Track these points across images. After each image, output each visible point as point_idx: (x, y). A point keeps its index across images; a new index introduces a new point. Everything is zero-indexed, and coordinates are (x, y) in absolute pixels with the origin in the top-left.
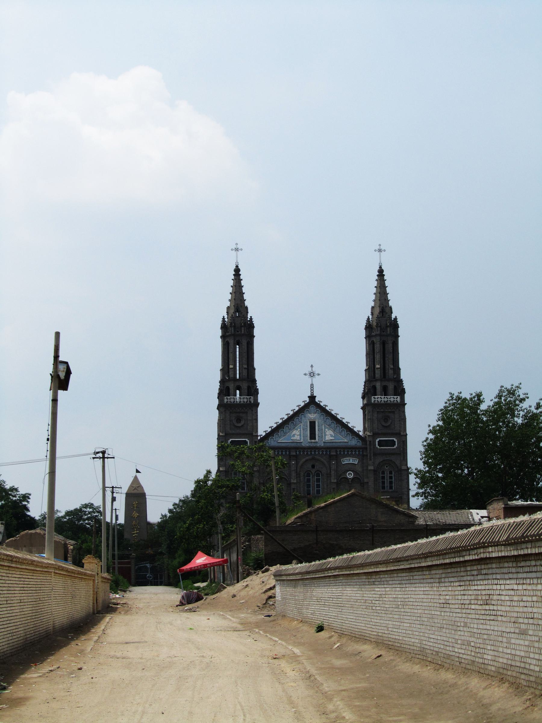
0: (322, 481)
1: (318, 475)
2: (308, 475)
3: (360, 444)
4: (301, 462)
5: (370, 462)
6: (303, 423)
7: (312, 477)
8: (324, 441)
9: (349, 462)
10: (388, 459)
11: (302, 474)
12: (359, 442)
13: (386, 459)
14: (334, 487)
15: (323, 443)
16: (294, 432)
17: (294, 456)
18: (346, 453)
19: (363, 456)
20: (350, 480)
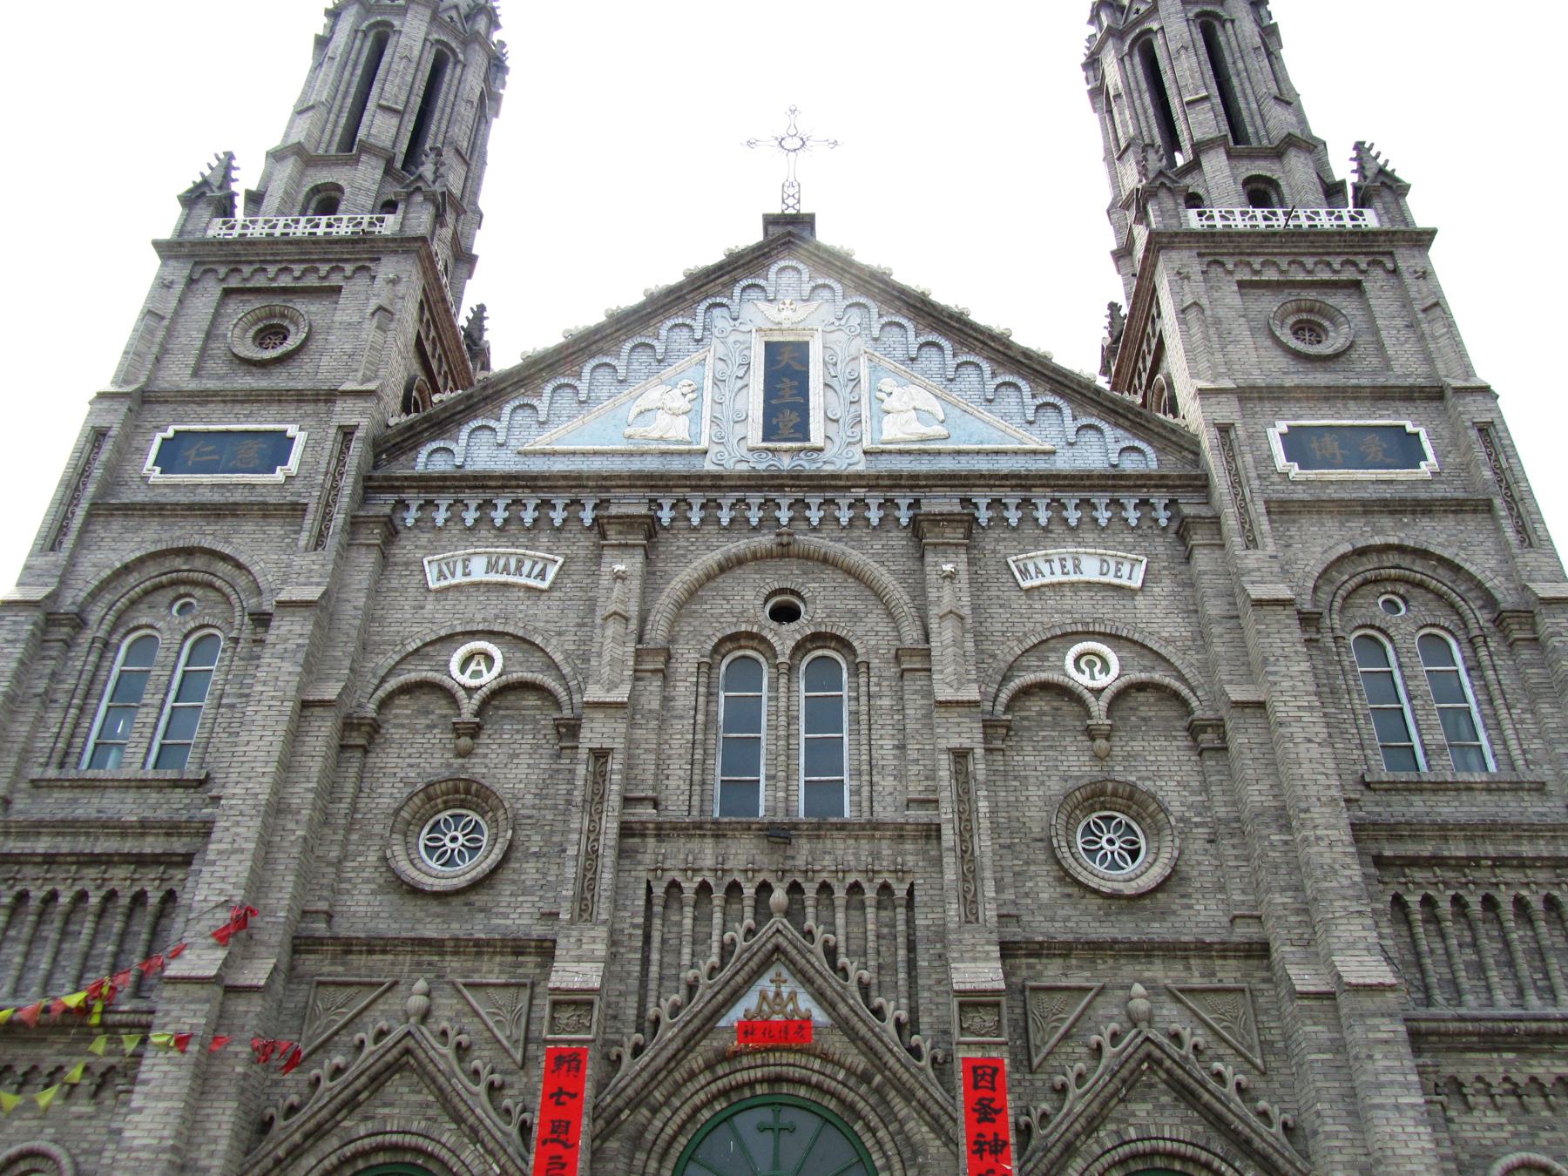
0: (855, 714)
1: (824, 674)
2: (745, 673)
4: (680, 579)
5: (1252, 559)
6: (716, 348)
7: (774, 687)
8: (866, 444)
9: (1074, 578)
10: (1394, 540)
11: (688, 657)
12: (1135, 456)
13: (1378, 540)
14: (966, 743)
15: (859, 456)
16: (653, 395)
17: (628, 522)
18: (1043, 516)
19: (1183, 530)
20: (1098, 707)
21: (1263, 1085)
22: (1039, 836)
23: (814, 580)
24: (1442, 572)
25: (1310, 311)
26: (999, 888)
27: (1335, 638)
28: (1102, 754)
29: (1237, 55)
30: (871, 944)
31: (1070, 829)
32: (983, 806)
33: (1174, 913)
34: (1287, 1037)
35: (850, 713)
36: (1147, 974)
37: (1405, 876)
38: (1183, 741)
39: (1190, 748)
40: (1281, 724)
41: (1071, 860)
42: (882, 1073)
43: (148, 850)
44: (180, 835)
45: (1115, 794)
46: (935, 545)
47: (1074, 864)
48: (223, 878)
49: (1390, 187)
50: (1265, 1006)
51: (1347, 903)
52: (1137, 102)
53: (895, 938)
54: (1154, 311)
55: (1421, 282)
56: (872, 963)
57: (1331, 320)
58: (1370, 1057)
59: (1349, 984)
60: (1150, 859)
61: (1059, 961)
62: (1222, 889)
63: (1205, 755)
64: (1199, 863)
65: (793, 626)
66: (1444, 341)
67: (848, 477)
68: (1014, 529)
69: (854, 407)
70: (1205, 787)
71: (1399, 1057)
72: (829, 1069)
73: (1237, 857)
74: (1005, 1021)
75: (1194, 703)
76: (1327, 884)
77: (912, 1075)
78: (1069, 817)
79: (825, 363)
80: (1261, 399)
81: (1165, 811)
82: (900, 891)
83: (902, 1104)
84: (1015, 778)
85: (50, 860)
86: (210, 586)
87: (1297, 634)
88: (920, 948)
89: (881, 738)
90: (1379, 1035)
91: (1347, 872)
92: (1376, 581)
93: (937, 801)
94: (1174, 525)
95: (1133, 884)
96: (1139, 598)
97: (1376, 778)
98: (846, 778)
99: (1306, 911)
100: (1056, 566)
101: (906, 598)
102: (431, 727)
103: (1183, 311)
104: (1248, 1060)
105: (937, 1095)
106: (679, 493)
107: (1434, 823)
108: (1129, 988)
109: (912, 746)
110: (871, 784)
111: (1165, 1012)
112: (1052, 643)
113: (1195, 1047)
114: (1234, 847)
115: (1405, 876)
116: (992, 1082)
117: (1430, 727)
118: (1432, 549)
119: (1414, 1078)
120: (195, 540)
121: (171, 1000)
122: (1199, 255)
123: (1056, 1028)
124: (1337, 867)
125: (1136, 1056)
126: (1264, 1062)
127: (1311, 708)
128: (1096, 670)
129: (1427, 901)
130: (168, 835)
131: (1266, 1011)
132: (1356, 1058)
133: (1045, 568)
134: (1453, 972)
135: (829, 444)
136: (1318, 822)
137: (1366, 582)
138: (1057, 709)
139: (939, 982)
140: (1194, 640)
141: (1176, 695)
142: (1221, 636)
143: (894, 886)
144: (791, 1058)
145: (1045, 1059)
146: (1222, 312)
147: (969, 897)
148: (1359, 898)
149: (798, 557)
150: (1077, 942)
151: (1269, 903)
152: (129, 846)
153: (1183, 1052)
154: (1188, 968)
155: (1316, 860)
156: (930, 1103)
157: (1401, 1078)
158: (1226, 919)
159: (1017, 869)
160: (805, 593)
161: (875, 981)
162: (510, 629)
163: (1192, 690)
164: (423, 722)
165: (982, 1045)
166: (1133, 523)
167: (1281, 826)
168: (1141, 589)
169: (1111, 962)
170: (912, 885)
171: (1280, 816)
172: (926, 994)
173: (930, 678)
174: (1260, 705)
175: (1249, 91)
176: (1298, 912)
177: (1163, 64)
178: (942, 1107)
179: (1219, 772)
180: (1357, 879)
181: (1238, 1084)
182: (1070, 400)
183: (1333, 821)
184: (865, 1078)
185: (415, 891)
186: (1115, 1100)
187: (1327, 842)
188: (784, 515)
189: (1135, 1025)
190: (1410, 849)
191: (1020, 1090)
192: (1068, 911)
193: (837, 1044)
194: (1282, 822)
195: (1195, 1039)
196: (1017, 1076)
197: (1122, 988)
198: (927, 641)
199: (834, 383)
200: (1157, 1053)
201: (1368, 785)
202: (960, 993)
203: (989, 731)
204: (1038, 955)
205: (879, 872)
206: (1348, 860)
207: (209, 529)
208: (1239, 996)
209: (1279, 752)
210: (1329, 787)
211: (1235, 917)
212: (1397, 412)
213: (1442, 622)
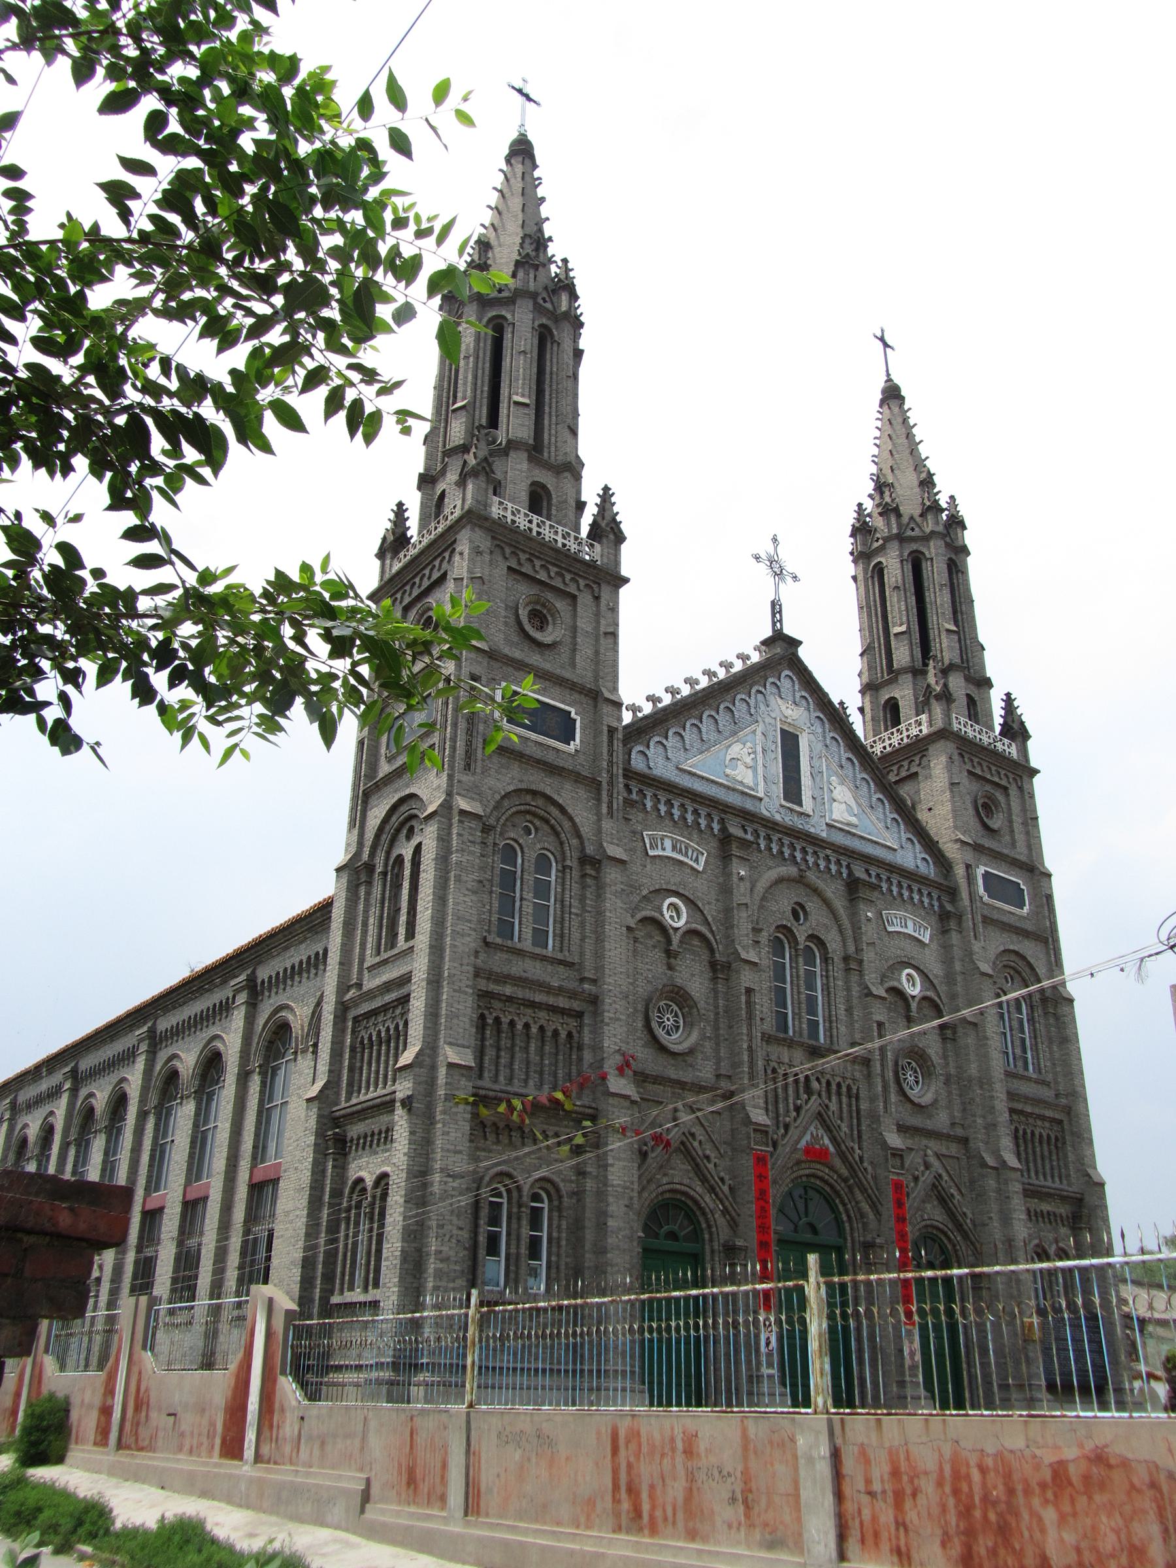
3: (928, 870)
10: (1016, 948)
15: (824, 827)
16: (736, 750)
24: (1027, 969)
43: (561, 1005)
44: (576, 999)
48: (615, 1035)
57: (996, 807)
72: (831, 1174)
85: (510, 999)
86: (547, 822)
88: (863, 1120)
102: (654, 947)
106: (756, 826)
120: (541, 787)
121: (613, 1106)
130: (570, 998)
144: (818, 1166)
152: (551, 1000)
162: (687, 894)
164: (650, 942)
184: (845, 1180)
185: (662, 1049)
193: (837, 1162)
207: (548, 780)
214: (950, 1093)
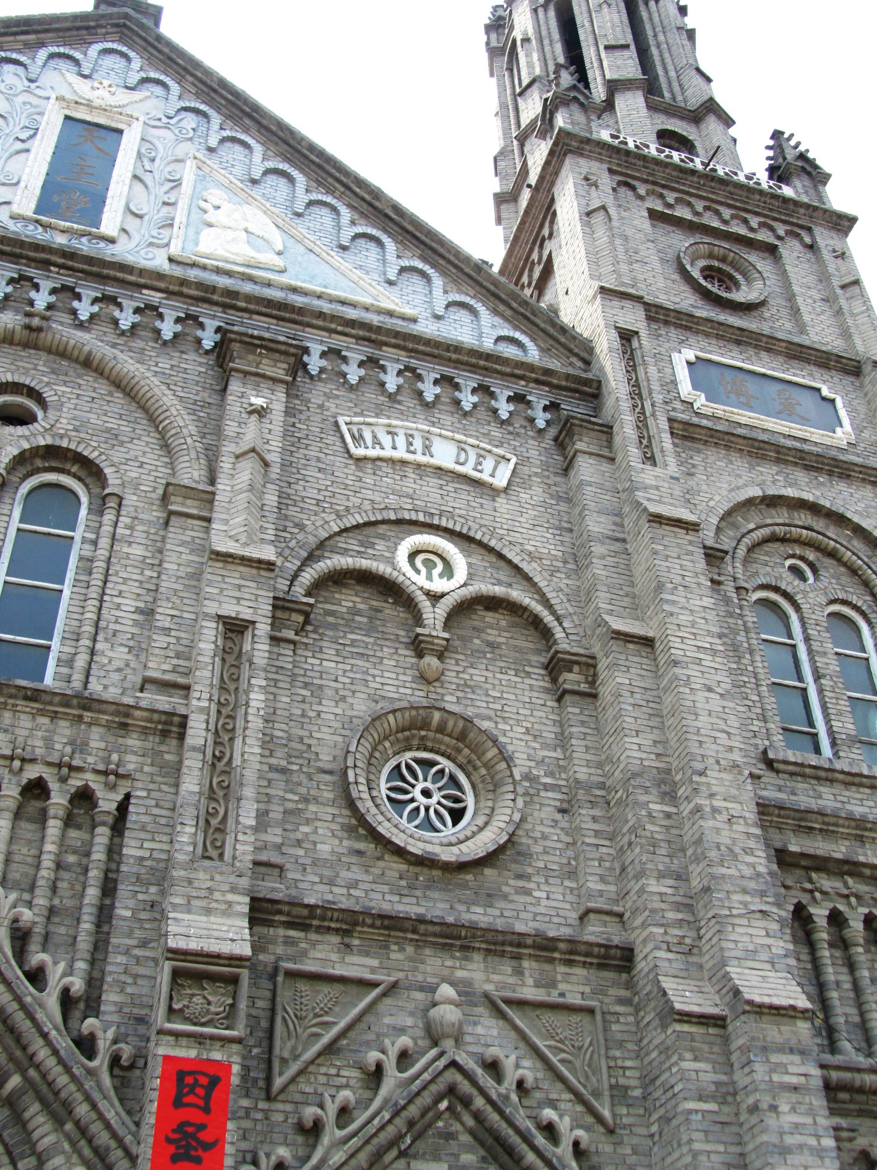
5: (648, 475)
8: (175, 249)
13: (790, 492)
14: (246, 614)
21: (608, 1148)
22: (328, 766)
23: (65, 383)
25: (723, 260)
26: (262, 821)
27: (738, 588)
28: (431, 675)
29: (659, 29)
30: (46, 873)
31: (372, 764)
32: (257, 699)
33: (505, 897)
34: (648, 1081)
35: (81, 558)
36: (460, 974)
37: (810, 881)
38: (538, 679)
39: (547, 691)
40: (676, 663)
41: (369, 804)
42: (23, 1073)
45: (441, 729)
46: (246, 373)
47: (374, 810)
49: (809, 174)
50: (619, 1036)
51: (748, 898)
52: (547, 49)
53: (86, 870)
54: (546, 232)
55: (839, 261)
56: (41, 901)
57: (744, 275)
58: (774, 1108)
59: (750, 1003)
60: (480, 821)
61: (335, 939)
62: (572, 874)
63: (568, 698)
64: (544, 837)
65: (20, 430)
66: (861, 319)
67: (142, 272)
68: (352, 388)
69: (166, 209)
70: (563, 741)
71: (811, 1112)
73: (597, 834)
74: (243, 1005)
75: (559, 634)
76: (723, 871)
77: (74, 1078)
78: (374, 749)
79: (139, 155)
80: (666, 323)
81: (508, 759)
82: (108, 802)
83: (48, 1127)
84: (306, 685)
87: (701, 564)
88: (124, 890)
89: (120, 594)
90: (787, 1079)
91: (750, 859)
92: (783, 540)
93: (187, 688)
94: (553, 432)
95: (455, 850)
96: (501, 500)
97: (781, 757)
98: (55, 644)
99: (689, 908)
100: (401, 441)
101: (193, 429)
103: (588, 214)
104: (591, 1110)
105: (110, 1115)
107: (850, 818)
108: (433, 989)
109: (164, 610)
110: (92, 652)
111: (480, 1030)
112: (382, 529)
113: (520, 1084)
114: (594, 819)
115: (810, 881)
116: (207, 1099)
117: (840, 713)
118: (849, 515)
119: (829, 1142)
122: (611, 171)
123: (317, 1036)
124: (737, 850)
125: (434, 1088)
126: (614, 1115)
127: (714, 652)
128: (436, 572)
129: (836, 919)
131: (621, 1044)
132: (754, 1109)
133: (386, 440)
134: (862, 1014)
135: (124, 236)
136: (715, 789)
137: (773, 538)
138: (377, 610)
139: (144, 944)
140: (565, 562)
141: (536, 622)
142: (603, 557)
143: (99, 794)
145: (293, 1080)
146: (629, 232)
147: (214, 822)
148: (763, 894)
149: (49, 351)
150: (366, 913)
151: (642, 891)
153: (502, 1090)
154: (519, 972)
155: (710, 837)
156: (96, 1128)
157: (812, 1142)
158: (575, 915)
159: (290, 806)
160: (48, 394)
161: (38, 929)
163: (558, 619)
165: (199, 1039)
166: (504, 415)
167: (665, 793)
168: (506, 490)
169: (410, 949)
170: (128, 796)
171: (663, 782)
172: (120, 959)
173: (207, 530)
174: (648, 642)
175: (668, 60)
176: (678, 907)
177: (581, 19)
178: (114, 1135)
179: (583, 723)
180: (762, 869)
181: (576, 1144)
182: (443, 273)
183: (734, 792)
186: (394, 1153)
187: (725, 817)
188: (42, 299)
189: (435, 1044)
190: (820, 847)
191: (247, 1124)
192: (356, 873)
194: (667, 789)
195: (520, 1072)
196: (245, 1103)
197: (421, 989)
198: (212, 481)
199: (147, 178)
200: (465, 1087)
201: (770, 764)
202: (176, 954)
203: (279, 614)
204: (304, 927)
205: (79, 769)
206: (752, 844)
208: (586, 1019)
209: (668, 699)
210: (731, 749)
211: (588, 911)
212: (811, 375)
213: (854, 600)
214: (574, 832)
